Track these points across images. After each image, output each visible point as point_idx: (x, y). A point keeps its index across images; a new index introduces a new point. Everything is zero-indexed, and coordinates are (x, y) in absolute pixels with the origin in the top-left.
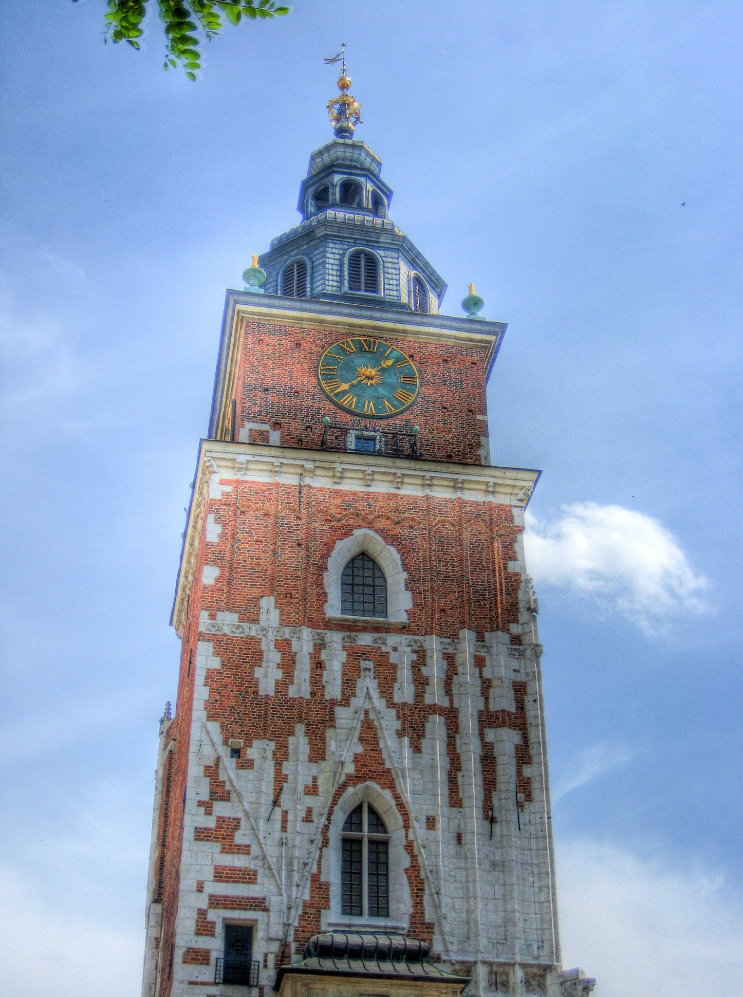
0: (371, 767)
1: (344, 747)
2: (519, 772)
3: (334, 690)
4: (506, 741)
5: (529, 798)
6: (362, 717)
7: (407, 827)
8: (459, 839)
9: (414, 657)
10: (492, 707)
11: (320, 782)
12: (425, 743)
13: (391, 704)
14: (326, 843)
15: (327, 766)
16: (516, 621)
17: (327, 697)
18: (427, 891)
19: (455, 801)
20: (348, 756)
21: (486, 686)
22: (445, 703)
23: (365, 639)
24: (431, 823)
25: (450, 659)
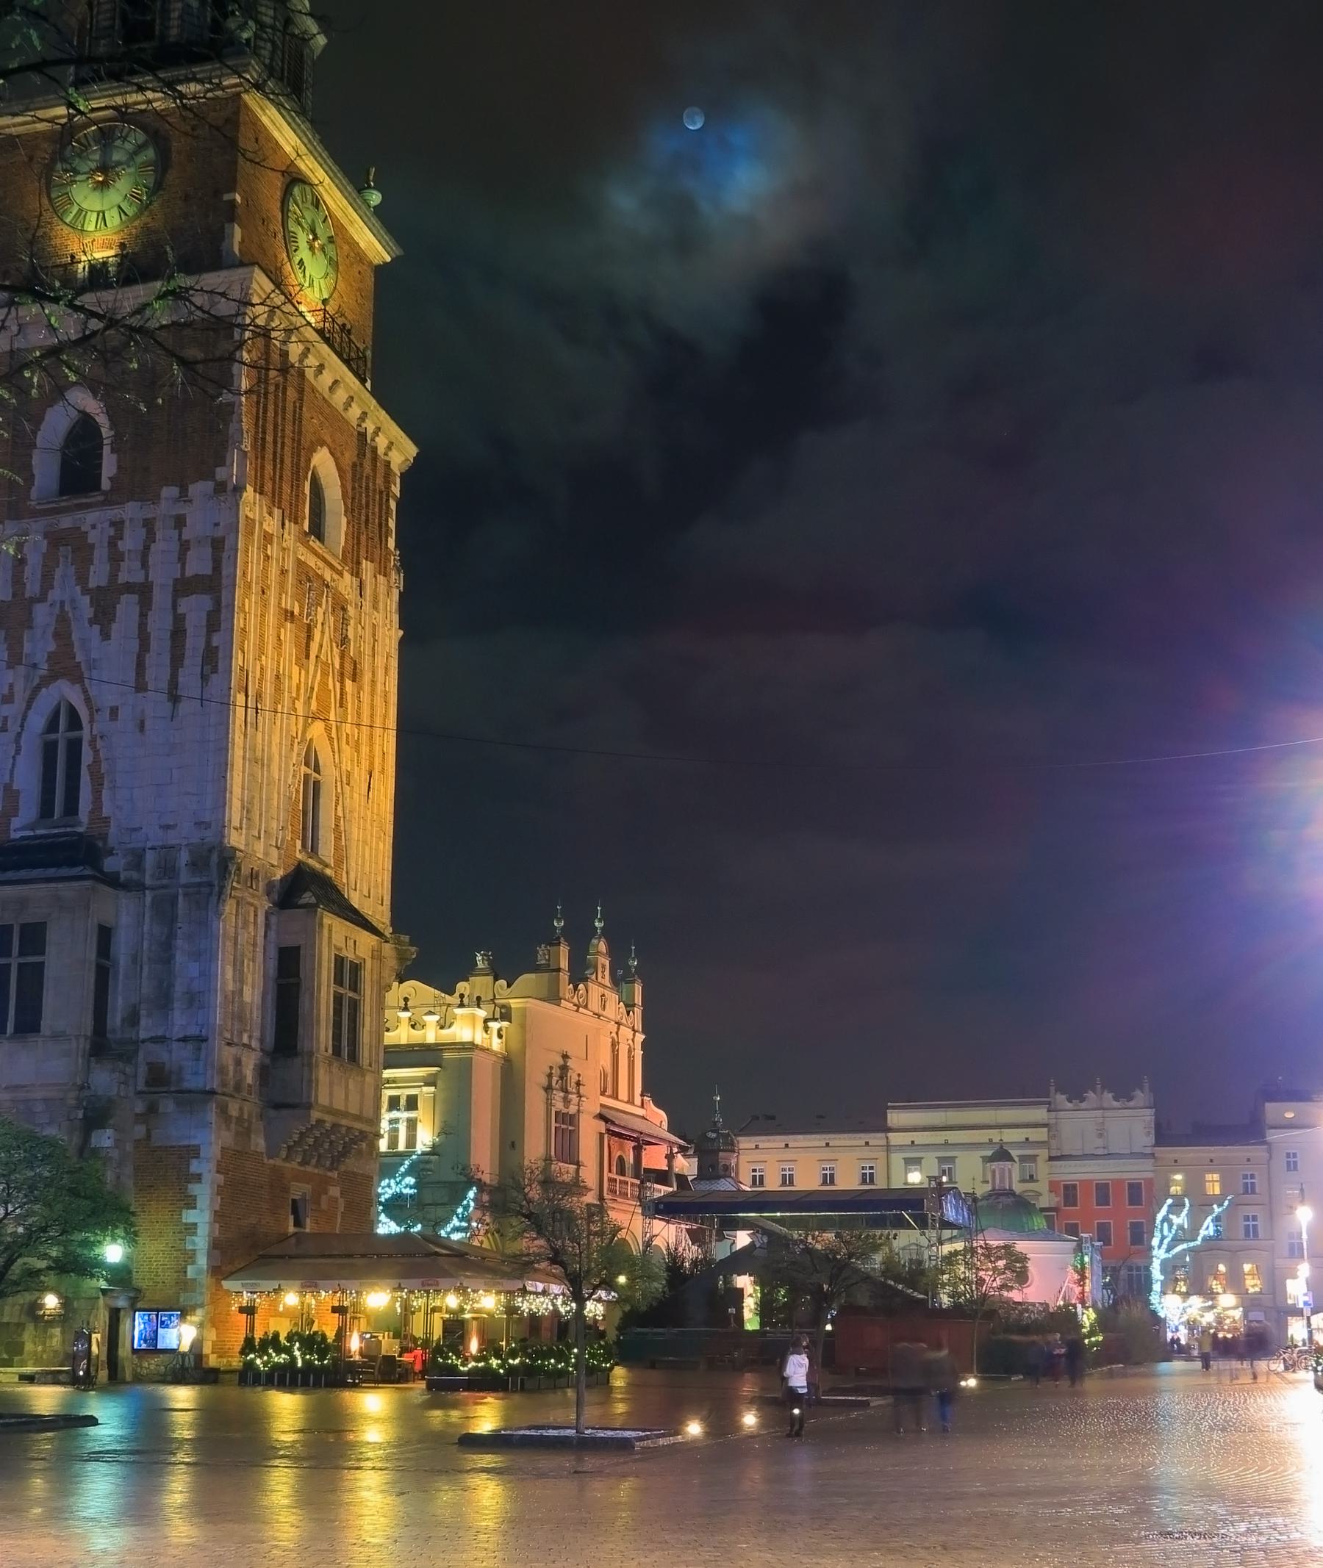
0: (65, 666)
1: (39, 646)
2: (208, 642)
3: (32, 588)
4: (195, 608)
5: (215, 670)
6: (57, 610)
7: (91, 721)
8: (142, 727)
9: (112, 532)
10: (189, 573)
11: (16, 689)
12: (114, 626)
13: (86, 591)
14: (18, 751)
15: (21, 669)
16: (223, 464)
17: (27, 595)
18: (105, 786)
19: (141, 687)
20: (41, 658)
21: (184, 547)
22: (138, 577)
23: (66, 522)
24: (114, 712)
25: (149, 524)
